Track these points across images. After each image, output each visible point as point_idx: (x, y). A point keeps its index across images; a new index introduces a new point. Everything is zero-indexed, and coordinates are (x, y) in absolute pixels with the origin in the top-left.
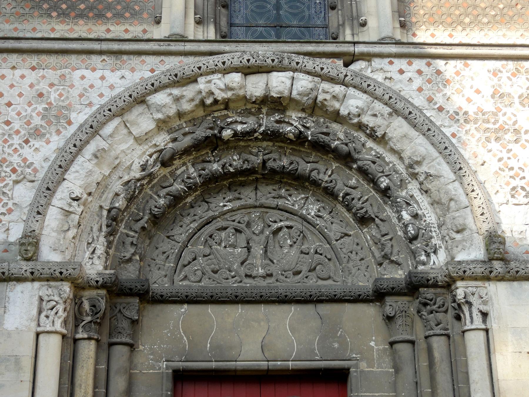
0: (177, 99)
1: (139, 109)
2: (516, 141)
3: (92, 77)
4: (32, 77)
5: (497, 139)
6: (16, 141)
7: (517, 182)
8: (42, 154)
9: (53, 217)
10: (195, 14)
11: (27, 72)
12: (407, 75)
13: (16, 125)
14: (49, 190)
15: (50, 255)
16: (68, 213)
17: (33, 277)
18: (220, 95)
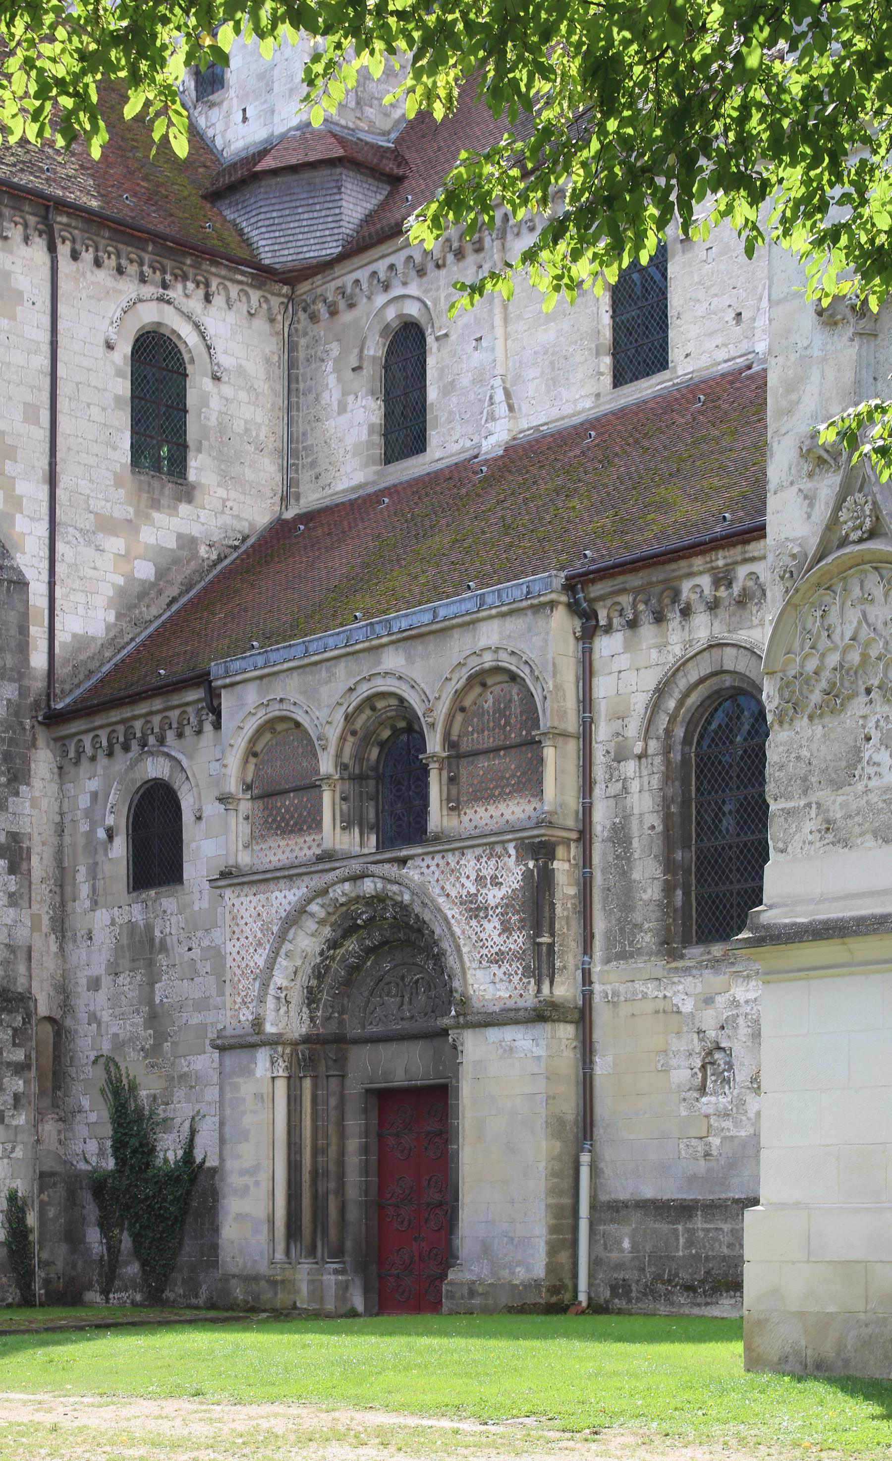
0: (322, 906)
1: (304, 917)
2: (486, 917)
3: (280, 895)
4: (255, 900)
5: (476, 916)
6: (252, 950)
7: (484, 951)
8: (260, 959)
9: (270, 1002)
10: (342, 822)
11: (251, 897)
12: (432, 868)
13: (250, 939)
14: (265, 986)
15: (270, 1029)
16: (278, 998)
17: (264, 1044)
18: (343, 900)
